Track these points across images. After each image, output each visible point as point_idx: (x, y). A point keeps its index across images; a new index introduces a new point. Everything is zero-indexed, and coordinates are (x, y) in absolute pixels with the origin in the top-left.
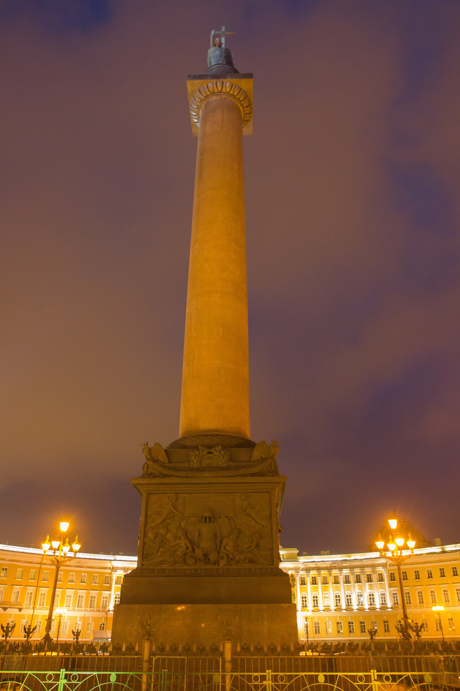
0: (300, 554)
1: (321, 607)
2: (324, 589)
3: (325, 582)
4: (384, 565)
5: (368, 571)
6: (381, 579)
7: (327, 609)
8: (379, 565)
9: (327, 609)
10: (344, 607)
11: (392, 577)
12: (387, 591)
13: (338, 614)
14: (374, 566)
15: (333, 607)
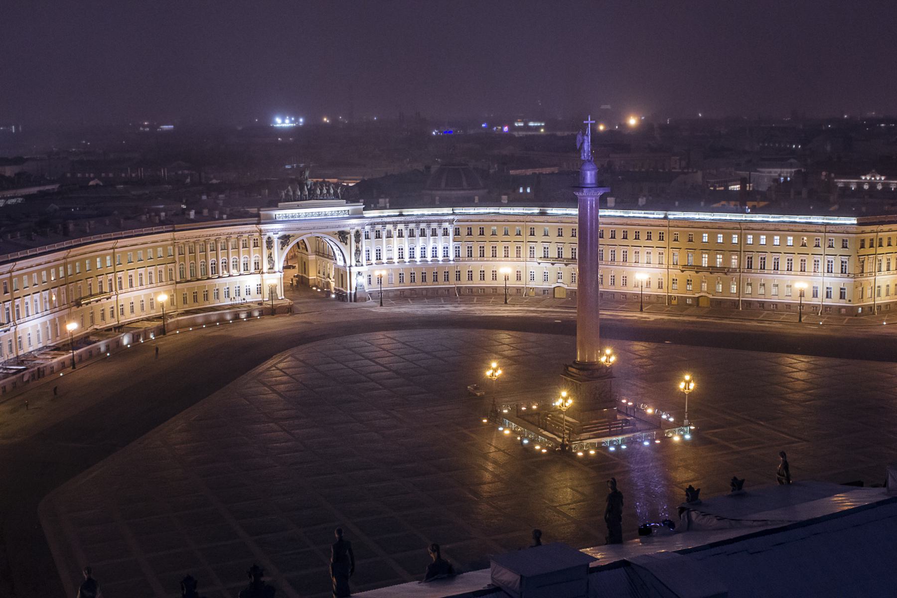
0: (364, 209)
1: (384, 260)
2: (388, 243)
3: (389, 236)
4: (451, 222)
5: (434, 225)
6: (446, 233)
7: (390, 261)
8: (446, 221)
9: (390, 261)
10: (407, 259)
11: (457, 232)
12: (452, 246)
13: (402, 266)
14: (440, 222)
15: (396, 260)
